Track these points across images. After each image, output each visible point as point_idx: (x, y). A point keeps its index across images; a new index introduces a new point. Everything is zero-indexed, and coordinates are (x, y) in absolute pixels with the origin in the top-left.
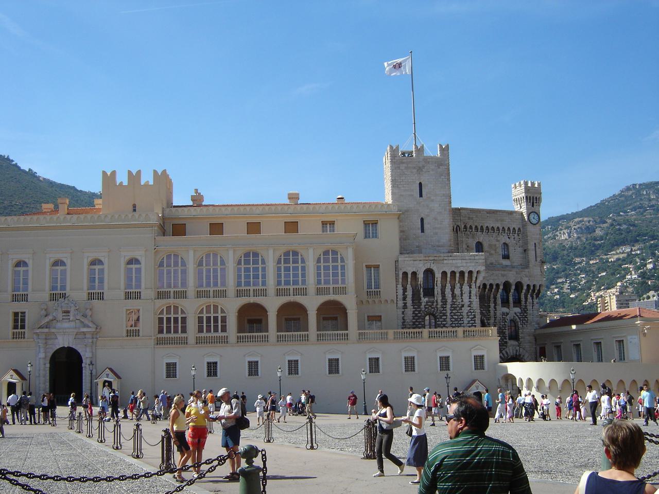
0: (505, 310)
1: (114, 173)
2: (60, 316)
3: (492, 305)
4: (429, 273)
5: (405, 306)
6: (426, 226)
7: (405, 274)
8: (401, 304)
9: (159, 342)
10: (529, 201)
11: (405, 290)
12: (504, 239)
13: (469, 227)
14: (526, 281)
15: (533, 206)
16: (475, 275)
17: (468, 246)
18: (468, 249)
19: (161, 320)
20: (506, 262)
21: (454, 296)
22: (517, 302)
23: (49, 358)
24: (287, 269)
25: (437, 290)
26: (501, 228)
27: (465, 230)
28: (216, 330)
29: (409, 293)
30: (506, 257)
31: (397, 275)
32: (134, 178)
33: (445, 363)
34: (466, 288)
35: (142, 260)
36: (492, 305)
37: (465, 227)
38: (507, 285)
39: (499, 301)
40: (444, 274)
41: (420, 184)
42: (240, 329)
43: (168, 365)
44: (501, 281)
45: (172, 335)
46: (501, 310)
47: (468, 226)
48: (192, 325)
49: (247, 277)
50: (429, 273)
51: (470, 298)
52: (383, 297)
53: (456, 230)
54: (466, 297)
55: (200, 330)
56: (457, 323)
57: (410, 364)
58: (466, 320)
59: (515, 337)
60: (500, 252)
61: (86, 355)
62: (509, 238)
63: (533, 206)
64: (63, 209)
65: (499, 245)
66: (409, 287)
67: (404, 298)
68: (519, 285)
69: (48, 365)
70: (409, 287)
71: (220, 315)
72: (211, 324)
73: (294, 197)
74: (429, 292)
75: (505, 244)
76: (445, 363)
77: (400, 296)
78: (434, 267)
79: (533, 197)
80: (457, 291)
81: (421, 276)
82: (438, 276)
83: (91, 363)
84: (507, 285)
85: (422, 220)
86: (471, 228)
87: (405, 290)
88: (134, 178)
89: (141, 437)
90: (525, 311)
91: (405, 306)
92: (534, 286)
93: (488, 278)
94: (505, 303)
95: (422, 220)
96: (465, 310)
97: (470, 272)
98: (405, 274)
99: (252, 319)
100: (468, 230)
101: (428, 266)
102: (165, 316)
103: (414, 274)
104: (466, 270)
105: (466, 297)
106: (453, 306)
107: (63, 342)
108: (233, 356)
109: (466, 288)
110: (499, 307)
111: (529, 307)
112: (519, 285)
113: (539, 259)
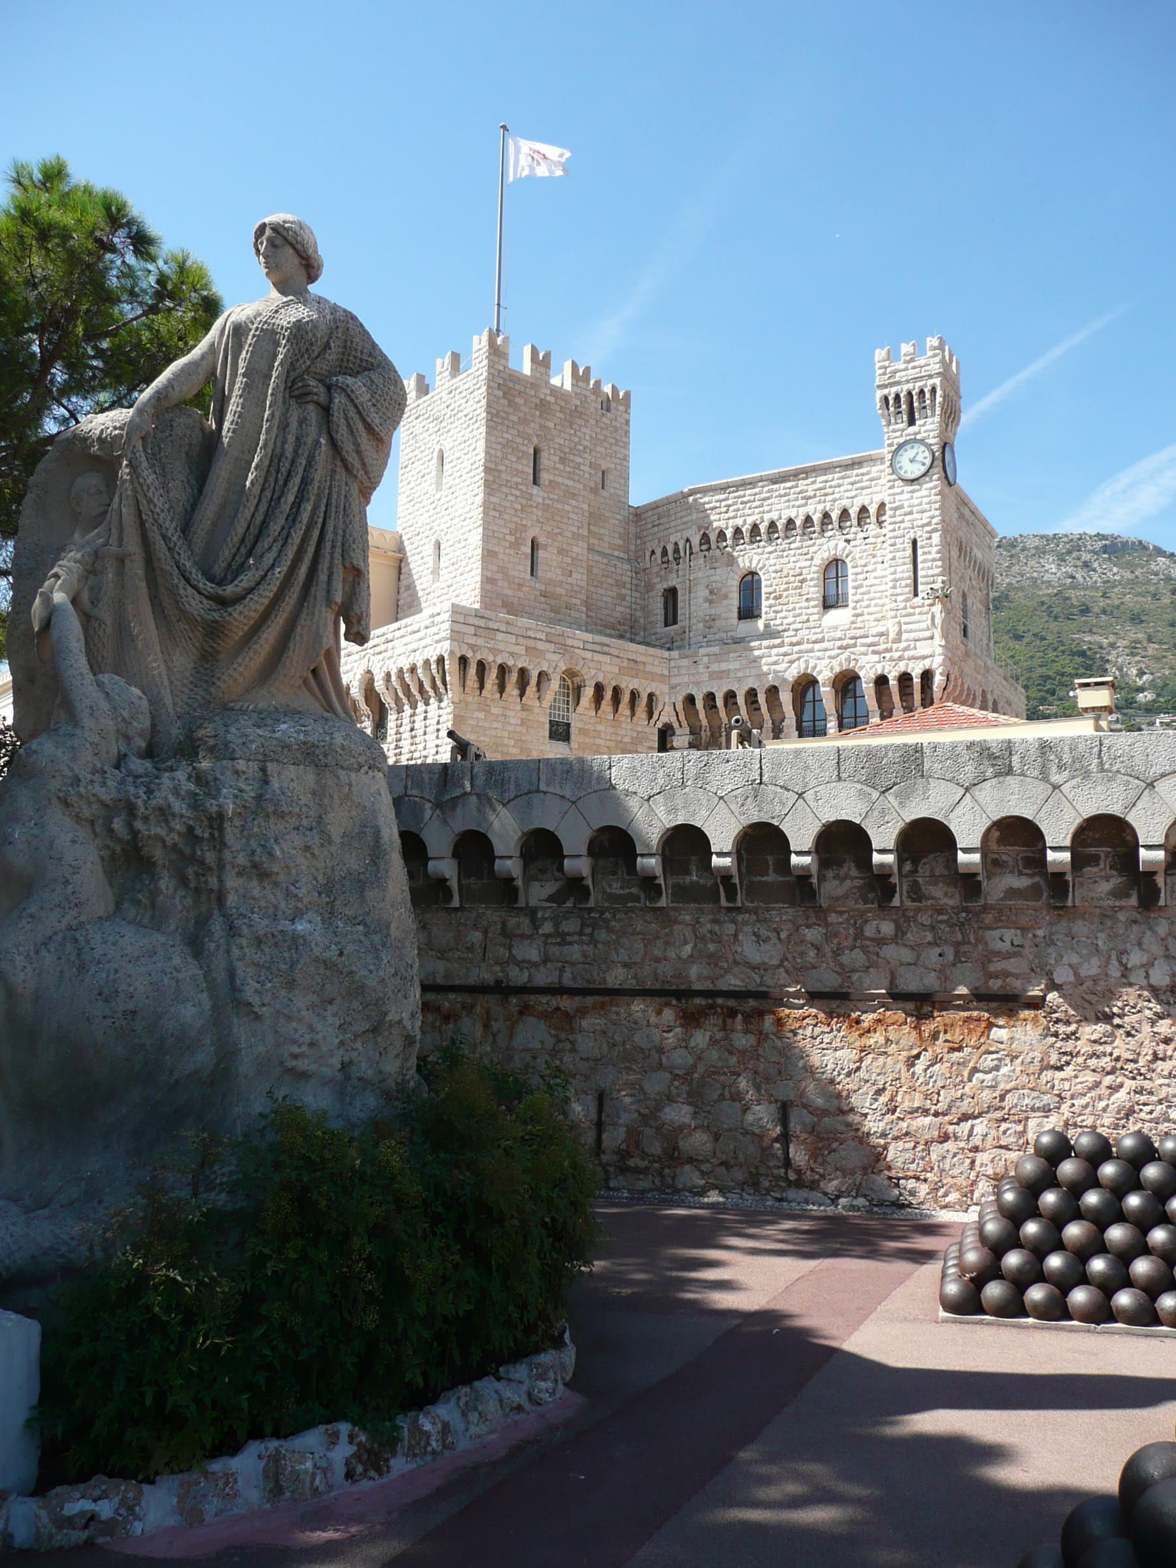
10: (892, 409)
12: (828, 546)
15: (912, 422)
17: (711, 592)
20: (834, 615)
26: (816, 518)
27: (704, 547)
37: (705, 539)
47: (713, 537)
60: (813, 591)
62: (848, 541)
63: (912, 422)
65: (813, 572)
79: (910, 394)
85: (438, 546)
86: (722, 535)
92: (905, 678)
93: (740, 674)
100: (713, 546)
112: (846, 683)
113: (920, 588)
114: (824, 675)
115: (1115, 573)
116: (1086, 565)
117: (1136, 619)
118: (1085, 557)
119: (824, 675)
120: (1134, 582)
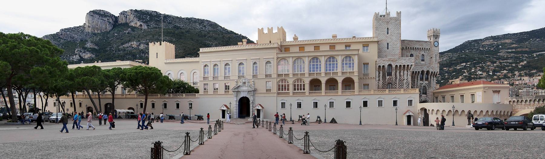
0: (422, 82)
1: (262, 29)
3: (416, 80)
5: (379, 80)
6: (389, 47)
7: (380, 66)
8: (377, 79)
9: (278, 94)
11: (379, 73)
12: (423, 53)
13: (407, 47)
14: (431, 71)
16: (410, 66)
18: (407, 56)
19: (279, 85)
21: (400, 75)
22: (427, 79)
24: (330, 65)
25: (393, 73)
28: (301, 90)
29: (381, 75)
30: (423, 60)
32: (270, 30)
33: (395, 103)
34: (406, 72)
35: (272, 62)
36: (416, 80)
38: (423, 72)
39: (419, 79)
40: (396, 66)
42: (311, 89)
44: (420, 70)
45: (284, 91)
46: (420, 82)
48: (291, 87)
49: (314, 68)
50: (390, 65)
51: (407, 77)
52: (370, 77)
53: (402, 49)
54: (405, 75)
55: (295, 90)
56: (401, 86)
57: (380, 103)
58: (405, 86)
59: (425, 93)
60: (421, 58)
61: (251, 99)
64: (245, 43)
65: (420, 55)
66: (381, 72)
67: (379, 77)
68: (428, 72)
70: (381, 72)
71: (302, 83)
72: (298, 87)
73: (334, 37)
74: (390, 74)
75: (423, 55)
76: (395, 103)
77: (377, 76)
80: (402, 74)
81: (386, 67)
82: (394, 66)
83: (253, 103)
84: (423, 72)
87: (379, 73)
88: (270, 30)
89: (190, 139)
90: (430, 83)
91: (379, 80)
94: (422, 79)
96: (405, 81)
97: (408, 66)
98: (380, 66)
99: (315, 84)
101: (389, 63)
102: (281, 84)
103: (383, 66)
104: (406, 65)
105: (405, 75)
106: (400, 80)
107: (242, 95)
108: (308, 100)
109: (406, 72)
110: (419, 81)
111: (432, 81)
112: (428, 72)
114: (425, 70)
115: (210, 28)
116: (205, 26)
117: (215, 39)
118: (205, 24)
119: (425, 70)
120: (214, 31)
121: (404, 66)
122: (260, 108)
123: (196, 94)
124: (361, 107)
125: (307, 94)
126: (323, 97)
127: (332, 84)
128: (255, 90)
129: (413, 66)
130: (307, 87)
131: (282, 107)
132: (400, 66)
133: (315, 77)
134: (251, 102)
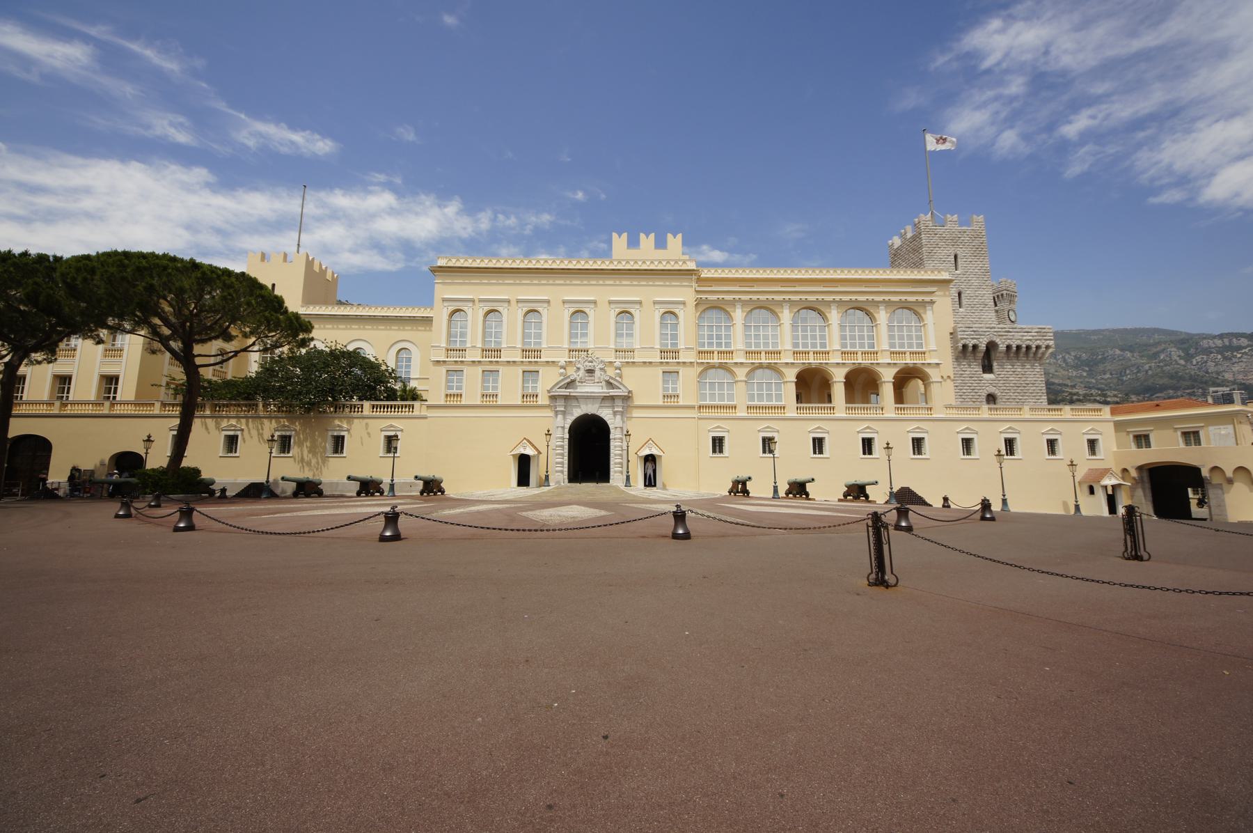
2: (581, 373)
4: (991, 346)
6: (964, 301)
7: (965, 346)
23: (567, 426)
31: (954, 348)
35: (681, 314)
40: (1009, 347)
41: (956, 257)
43: (714, 439)
61: (613, 422)
69: (567, 436)
78: (998, 341)
85: (960, 294)
95: (960, 294)
97: (1038, 347)
103: (975, 347)
121: (1028, 348)
122: (655, 452)
123: (417, 404)
124: (999, 454)
125: (791, 412)
126: (841, 421)
127: (862, 384)
128: (627, 398)
129: (1050, 350)
130: (790, 391)
131: (714, 451)
132: (1018, 347)
133: (812, 360)
134: (614, 434)
